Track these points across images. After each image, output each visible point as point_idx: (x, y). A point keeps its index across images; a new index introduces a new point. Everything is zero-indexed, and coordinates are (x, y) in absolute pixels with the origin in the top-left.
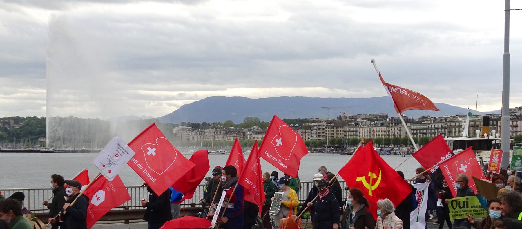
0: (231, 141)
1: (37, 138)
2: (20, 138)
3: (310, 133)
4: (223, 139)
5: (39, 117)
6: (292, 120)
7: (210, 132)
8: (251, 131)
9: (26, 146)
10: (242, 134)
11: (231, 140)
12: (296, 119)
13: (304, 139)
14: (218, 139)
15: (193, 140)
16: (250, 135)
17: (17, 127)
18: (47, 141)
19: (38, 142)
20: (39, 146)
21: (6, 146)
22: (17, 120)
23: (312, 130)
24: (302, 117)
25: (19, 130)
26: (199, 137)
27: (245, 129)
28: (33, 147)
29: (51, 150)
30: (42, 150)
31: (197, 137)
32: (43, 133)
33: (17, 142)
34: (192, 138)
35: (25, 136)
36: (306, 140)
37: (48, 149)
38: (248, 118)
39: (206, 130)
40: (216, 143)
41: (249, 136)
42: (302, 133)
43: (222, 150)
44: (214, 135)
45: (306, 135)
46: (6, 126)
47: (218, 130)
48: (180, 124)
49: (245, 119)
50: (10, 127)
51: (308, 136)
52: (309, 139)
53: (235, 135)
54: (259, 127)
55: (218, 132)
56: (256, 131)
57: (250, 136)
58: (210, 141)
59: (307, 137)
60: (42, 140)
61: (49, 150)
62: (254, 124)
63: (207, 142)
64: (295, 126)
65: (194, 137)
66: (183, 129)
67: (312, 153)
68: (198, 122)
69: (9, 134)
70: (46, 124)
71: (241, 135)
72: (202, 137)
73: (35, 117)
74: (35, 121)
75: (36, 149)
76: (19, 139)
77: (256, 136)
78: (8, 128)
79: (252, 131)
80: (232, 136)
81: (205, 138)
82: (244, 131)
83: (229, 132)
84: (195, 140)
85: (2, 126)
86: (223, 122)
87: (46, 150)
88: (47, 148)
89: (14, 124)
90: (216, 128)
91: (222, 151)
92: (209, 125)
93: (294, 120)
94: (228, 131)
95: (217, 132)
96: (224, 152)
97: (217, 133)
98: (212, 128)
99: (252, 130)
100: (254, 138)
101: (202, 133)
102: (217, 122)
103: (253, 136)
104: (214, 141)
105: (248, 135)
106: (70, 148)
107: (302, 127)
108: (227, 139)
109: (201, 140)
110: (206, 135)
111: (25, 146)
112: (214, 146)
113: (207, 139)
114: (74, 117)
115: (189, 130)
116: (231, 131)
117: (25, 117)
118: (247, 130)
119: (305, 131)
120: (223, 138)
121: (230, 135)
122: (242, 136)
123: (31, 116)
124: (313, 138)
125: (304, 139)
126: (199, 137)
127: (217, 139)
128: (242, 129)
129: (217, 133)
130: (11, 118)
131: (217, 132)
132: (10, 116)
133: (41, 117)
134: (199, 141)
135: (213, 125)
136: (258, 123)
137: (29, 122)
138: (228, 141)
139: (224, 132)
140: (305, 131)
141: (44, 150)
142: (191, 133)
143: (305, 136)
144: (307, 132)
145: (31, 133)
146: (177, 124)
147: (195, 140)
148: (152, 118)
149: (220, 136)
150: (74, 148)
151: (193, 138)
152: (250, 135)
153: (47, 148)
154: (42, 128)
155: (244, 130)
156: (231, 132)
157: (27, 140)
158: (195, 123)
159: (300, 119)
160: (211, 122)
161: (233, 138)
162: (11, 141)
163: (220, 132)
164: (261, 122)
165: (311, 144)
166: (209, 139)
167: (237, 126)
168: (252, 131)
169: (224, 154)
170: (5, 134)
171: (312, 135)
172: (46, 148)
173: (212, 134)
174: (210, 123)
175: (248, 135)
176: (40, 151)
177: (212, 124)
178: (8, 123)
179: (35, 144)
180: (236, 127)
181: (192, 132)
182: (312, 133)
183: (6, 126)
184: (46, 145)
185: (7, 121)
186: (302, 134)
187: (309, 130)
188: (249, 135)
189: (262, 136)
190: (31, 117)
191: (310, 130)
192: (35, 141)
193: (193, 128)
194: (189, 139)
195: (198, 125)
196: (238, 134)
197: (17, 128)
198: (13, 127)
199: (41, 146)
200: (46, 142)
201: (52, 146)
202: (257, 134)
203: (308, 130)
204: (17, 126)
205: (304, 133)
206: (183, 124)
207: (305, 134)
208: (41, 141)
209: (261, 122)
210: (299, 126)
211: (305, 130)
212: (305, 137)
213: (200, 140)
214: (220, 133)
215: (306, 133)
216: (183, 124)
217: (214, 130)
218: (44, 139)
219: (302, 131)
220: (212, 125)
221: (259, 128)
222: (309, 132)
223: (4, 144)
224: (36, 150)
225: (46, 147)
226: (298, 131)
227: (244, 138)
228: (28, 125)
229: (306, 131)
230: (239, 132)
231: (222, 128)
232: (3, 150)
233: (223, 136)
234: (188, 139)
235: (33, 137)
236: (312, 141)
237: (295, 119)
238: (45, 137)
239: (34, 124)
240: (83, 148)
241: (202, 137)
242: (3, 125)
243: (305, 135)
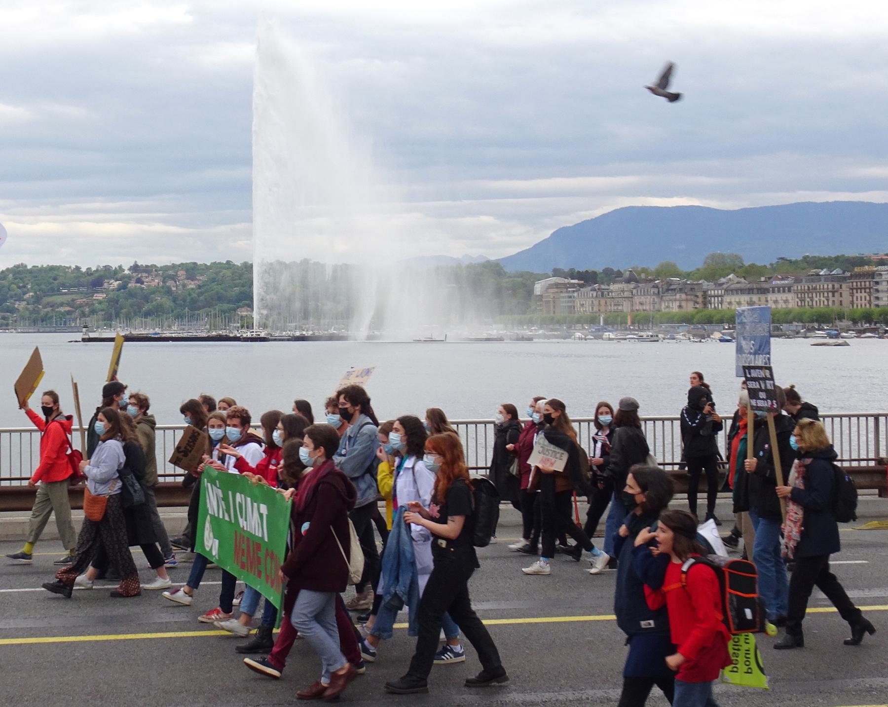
0: (674, 310)
1: (235, 310)
2: (199, 309)
3: (872, 290)
4: (654, 307)
5: (238, 263)
6: (824, 259)
7: (623, 291)
8: (721, 288)
9: (210, 326)
10: (700, 294)
11: (672, 308)
12: (835, 257)
13: (857, 305)
14: (641, 308)
15: (581, 309)
16: (720, 296)
17: (192, 285)
18: (256, 316)
19: (237, 318)
20: (238, 327)
21: (170, 326)
22: (192, 270)
23: (877, 283)
24: (852, 252)
25: (197, 291)
26: (596, 302)
27: (706, 283)
28: (224, 330)
29: (262, 335)
30: (245, 335)
31: (591, 302)
32: (246, 298)
33: (193, 318)
34: (578, 304)
35: (208, 304)
36: (863, 306)
37: (256, 332)
38: (713, 257)
39: (614, 287)
40: (636, 316)
41: (716, 298)
42: (852, 289)
43: (651, 334)
44: (630, 298)
45: (863, 294)
46: (170, 283)
47: (640, 285)
48: (550, 273)
49: (708, 258)
50: (177, 286)
51: (868, 298)
52: (870, 305)
53: (684, 296)
54: (740, 278)
55: (643, 291)
56: (733, 286)
57: (720, 299)
58: (622, 311)
59: (865, 300)
60: (244, 314)
61: (259, 335)
62: (730, 271)
63: (616, 314)
64: (833, 273)
65: (584, 303)
66: (557, 285)
67: (880, 338)
68: (591, 268)
69: (174, 301)
70: (253, 278)
71: (697, 296)
72: (603, 302)
73: (228, 262)
74: (228, 273)
75: (232, 333)
76: (196, 312)
77: (734, 298)
78: (174, 289)
79: (725, 286)
80: (676, 300)
81: (611, 305)
82: (705, 287)
83: (668, 290)
84: (587, 309)
85: (161, 284)
86: (653, 267)
87: (252, 335)
88: (254, 330)
89: (188, 278)
90: (637, 281)
91: (652, 336)
92: (619, 274)
93: (830, 259)
94: (665, 287)
95: (639, 291)
96: (655, 338)
97: (642, 294)
98: (628, 281)
99: (723, 284)
100: (730, 303)
101: (602, 294)
102: (637, 267)
103: (727, 299)
104: (632, 311)
105: (714, 296)
106: (303, 330)
107: (851, 277)
108: (663, 306)
109: (601, 311)
110: (613, 298)
111: (208, 327)
112: (633, 323)
113: (616, 308)
114: (311, 262)
115: (573, 285)
116: (672, 287)
117: (209, 264)
118: (713, 283)
119: (861, 285)
120: (654, 303)
121: (671, 298)
122: (700, 300)
123: (222, 262)
124: (881, 303)
125: (857, 305)
126: (596, 302)
127: (637, 307)
128: (700, 282)
129: (642, 294)
130: (179, 266)
131: (639, 291)
132: (178, 263)
133: (242, 262)
134: (596, 312)
135: (628, 273)
136: (741, 267)
137: (217, 273)
138: (667, 310)
139: (656, 291)
140: (859, 286)
141: (249, 335)
142: (576, 294)
143: (861, 297)
144: (865, 289)
145: (220, 298)
146: (545, 274)
147: (587, 309)
148: (486, 260)
149: (648, 299)
150: (312, 330)
151: (582, 305)
152: (720, 296)
153: (254, 330)
154: (243, 286)
155: (705, 284)
156: (672, 290)
157: (212, 313)
158: (587, 271)
159: (846, 256)
160: (625, 267)
161: (678, 303)
162: (180, 317)
163: (646, 290)
164: (747, 263)
165: (875, 317)
166: (620, 308)
167: (688, 275)
168: (725, 286)
169: (658, 341)
170: (167, 302)
171: (880, 295)
172: (253, 332)
173: (626, 294)
174: (622, 271)
175: (714, 296)
176: (239, 337)
177: (626, 271)
178: (174, 278)
179: (228, 322)
180: (685, 278)
181: (580, 292)
182: (877, 291)
183: (170, 283)
184: (253, 324)
185: (171, 272)
186: (853, 293)
187: (870, 281)
188: (718, 296)
189: (751, 299)
190: (220, 263)
191: (872, 283)
192: (228, 316)
193: (582, 282)
194: (571, 307)
195: (594, 274)
196: (689, 295)
197: (192, 289)
198: (184, 286)
199: (242, 327)
200: (253, 318)
201: (265, 326)
202: (737, 294)
203: (867, 283)
204: (192, 283)
205: (857, 289)
206: (557, 273)
207: (861, 292)
208: (242, 317)
209: (747, 265)
210: (844, 273)
211: (859, 284)
212: (861, 300)
213: (599, 310)
214: (646, 293)
215: (863, 291)
216: (557, 273)
217: (632, 285)
218: (247, 311)
219: (853, 286)
220: (627, 274)
221: (742, 280)
222: (870, 288)
223: (166, 324)
224: (231, 335)
225: (253, 329)
226: (841, 286)
227: (705, 304)
228: (213, 280)
229: (863, 286)
230: (690, 290)
231: (651, 281)
232: (164, 335)
233: (654, 299)
234: (572, 308)
235: (225, 306)
236: (878, 309)
237: (833, 256)
238: (251, 306)
239: (227, 279)
240: (332, 331)
241: (603, 302)
242: (164, 282)
243: (859, 295)
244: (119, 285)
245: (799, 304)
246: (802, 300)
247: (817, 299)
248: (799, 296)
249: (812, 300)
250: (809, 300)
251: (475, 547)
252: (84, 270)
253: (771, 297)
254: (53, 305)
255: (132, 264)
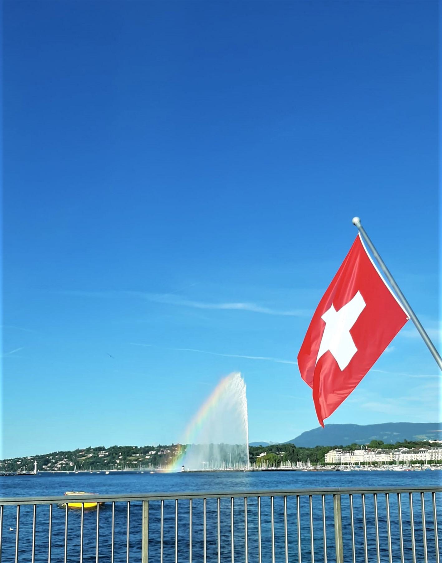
244: (155, 453)
245: (431, 457)
246: (432, 456)
247: (438, 455)
248: (431, 454)
249: (436, 455)
250: (434, 456)
251: (332, 306)
252: (139, 447)
253: (419, 455)
254: (130, 460)
255: (158, 445)
